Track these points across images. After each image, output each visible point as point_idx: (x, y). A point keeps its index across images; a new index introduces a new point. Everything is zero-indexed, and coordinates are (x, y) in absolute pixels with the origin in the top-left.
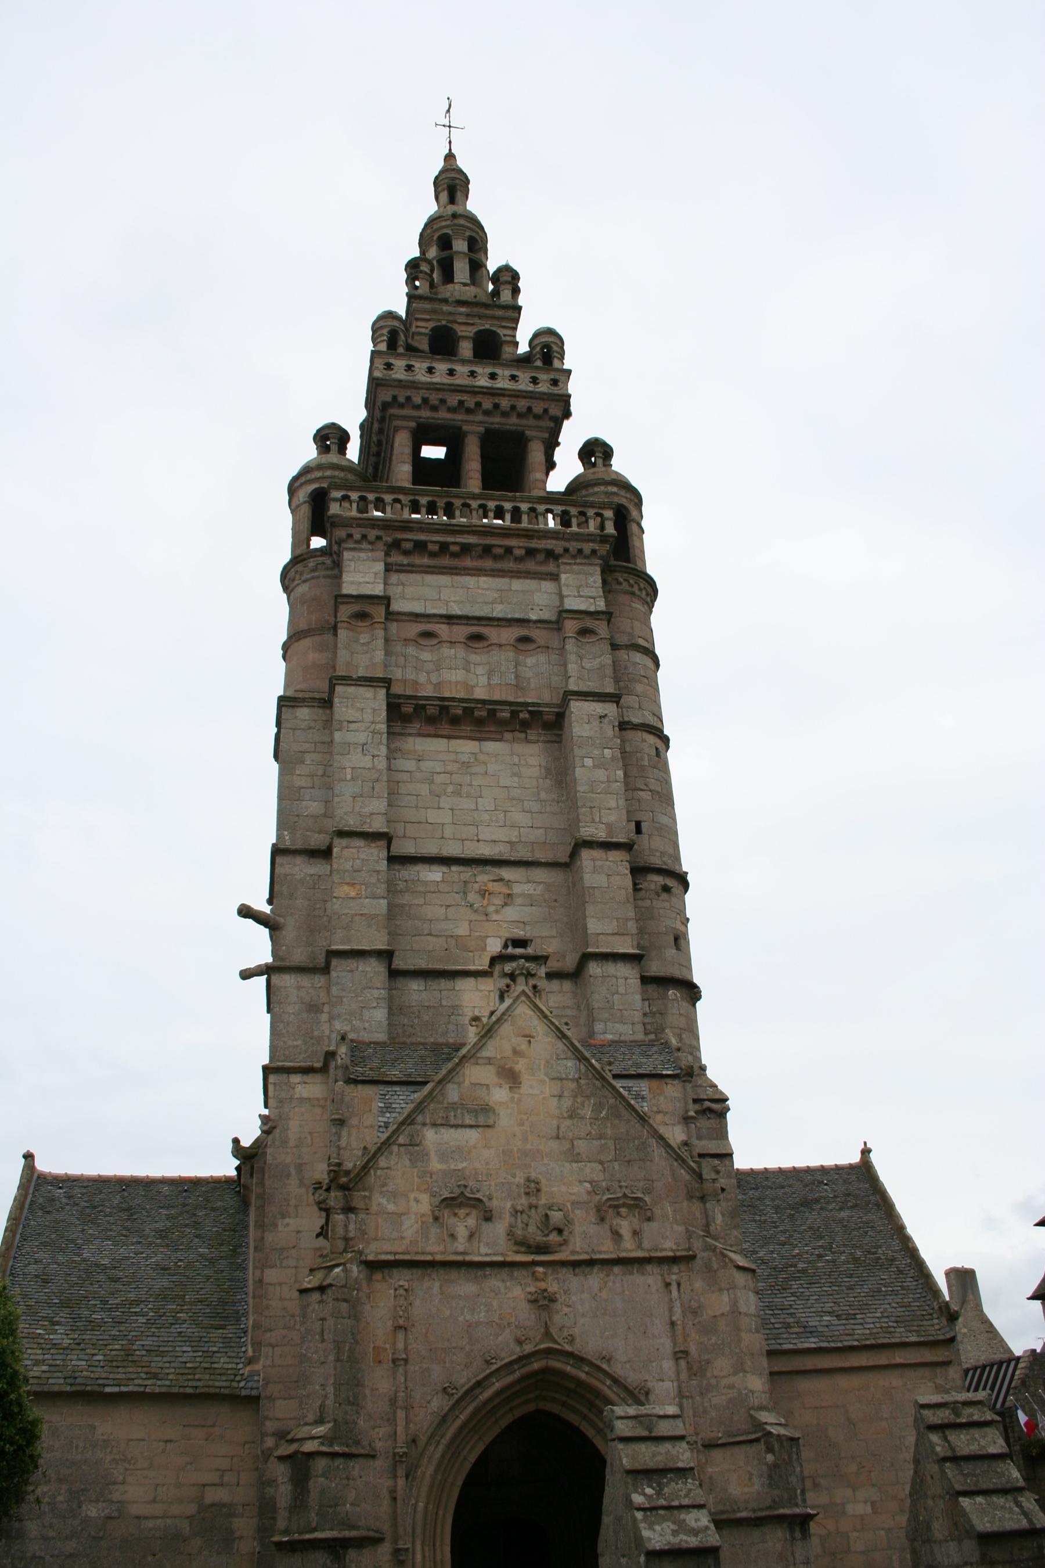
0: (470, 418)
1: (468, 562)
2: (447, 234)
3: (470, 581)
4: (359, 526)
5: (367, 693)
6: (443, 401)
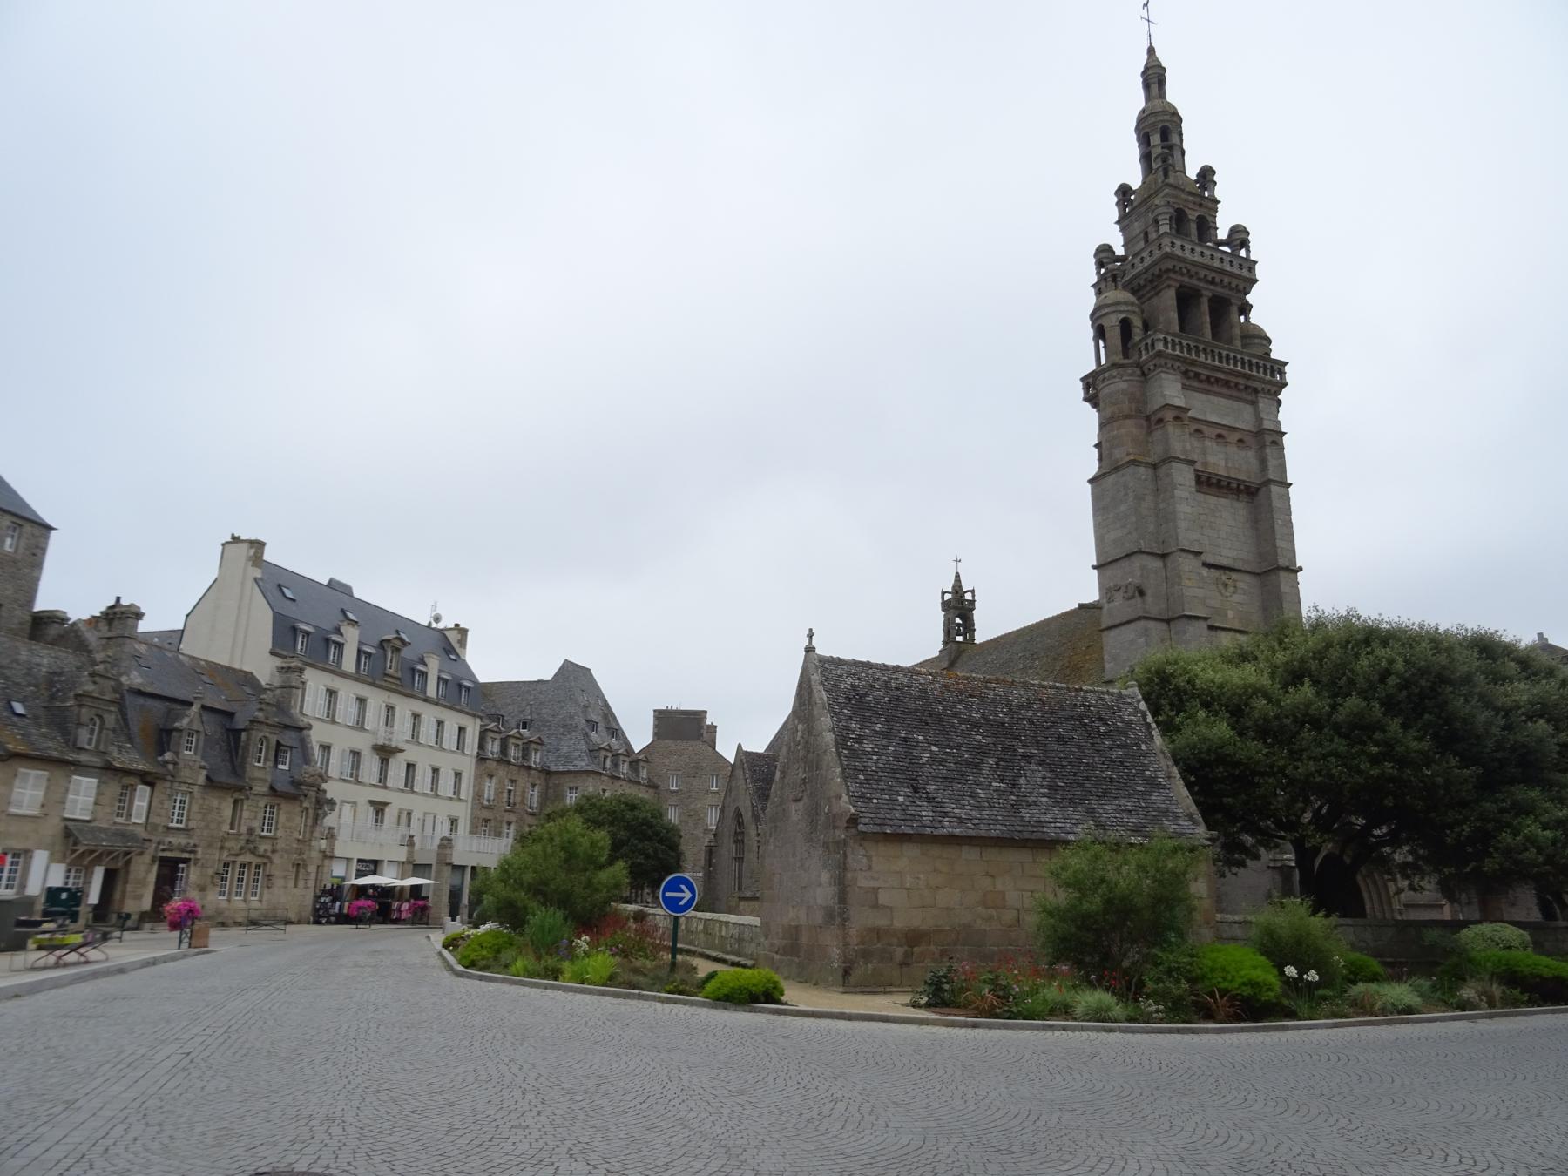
0: (1206, 286)
1: (1215, 388)
2: (1168, 127)
3: (1216, 399)
4: (1172, 359)
5: (1185, 467)
6: (1197, 273)
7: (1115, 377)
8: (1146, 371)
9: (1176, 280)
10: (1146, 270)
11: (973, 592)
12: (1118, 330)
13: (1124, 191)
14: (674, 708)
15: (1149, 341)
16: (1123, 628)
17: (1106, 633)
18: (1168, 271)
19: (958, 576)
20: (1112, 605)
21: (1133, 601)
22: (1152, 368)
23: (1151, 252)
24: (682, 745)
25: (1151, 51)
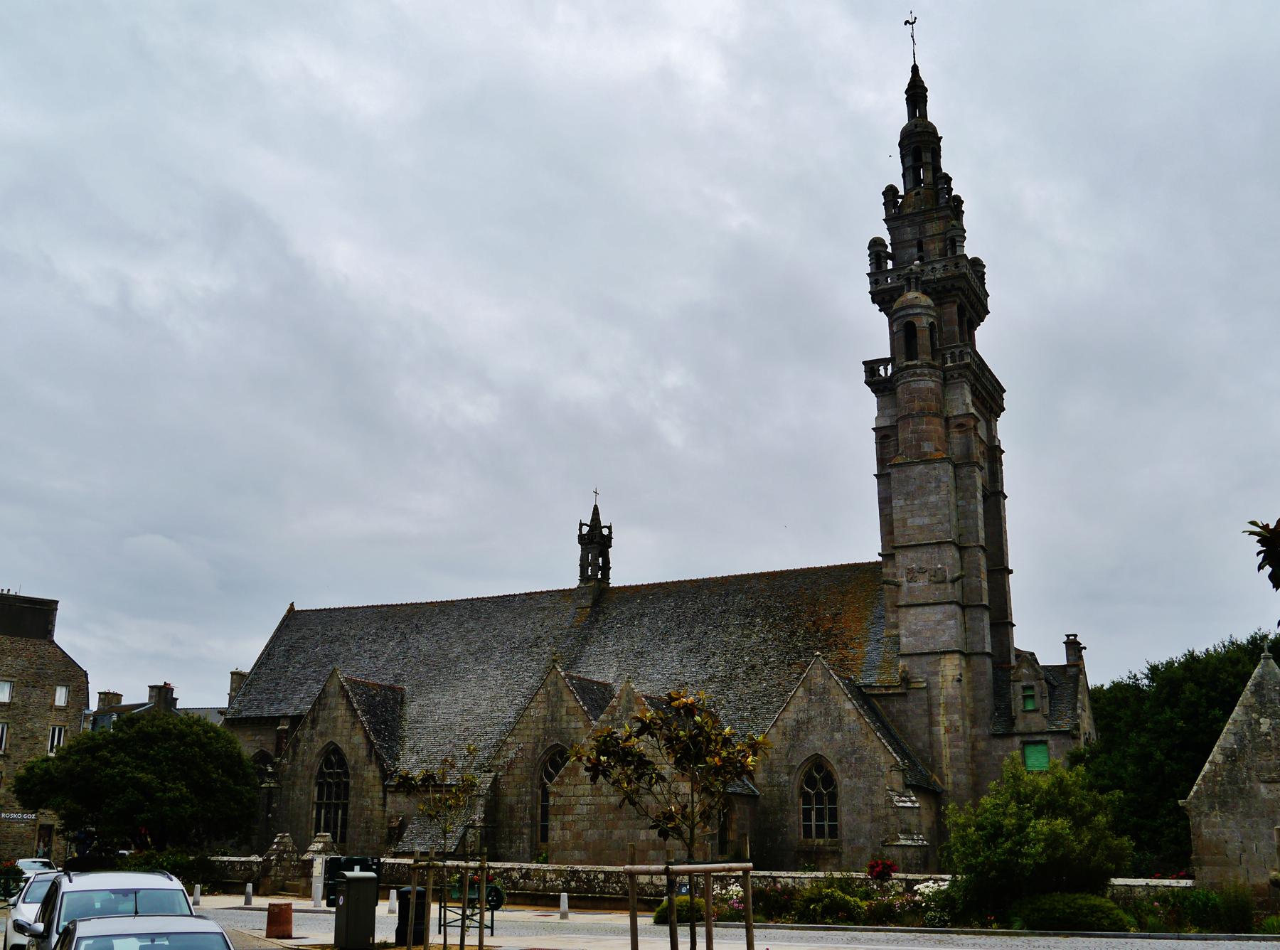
7: (925, 375)
8: (948, 377)
9: (960, 299)
10: (939, 280)
11: (610, 528)
12: (927, 333)
13: (890, 192)
14: (12, 593)
15: (957, 351)
16: (927, 609)
17: (904, 610)
18: (959, 289)
19: (596, 508)
20: (911, 585)
21: (942, 586)
22: (956, 375)
23: (945, 266)
24: (21, 644)
25: (915, 69)
